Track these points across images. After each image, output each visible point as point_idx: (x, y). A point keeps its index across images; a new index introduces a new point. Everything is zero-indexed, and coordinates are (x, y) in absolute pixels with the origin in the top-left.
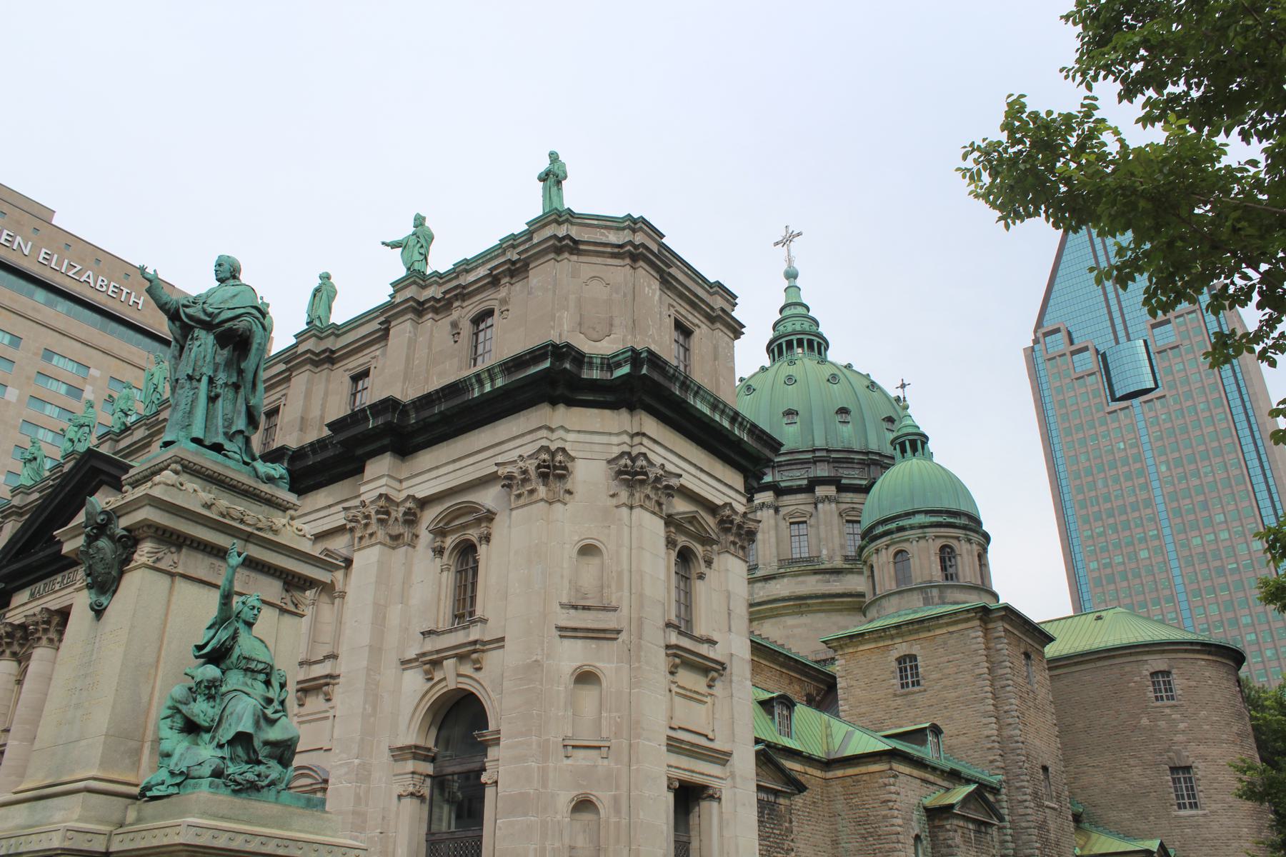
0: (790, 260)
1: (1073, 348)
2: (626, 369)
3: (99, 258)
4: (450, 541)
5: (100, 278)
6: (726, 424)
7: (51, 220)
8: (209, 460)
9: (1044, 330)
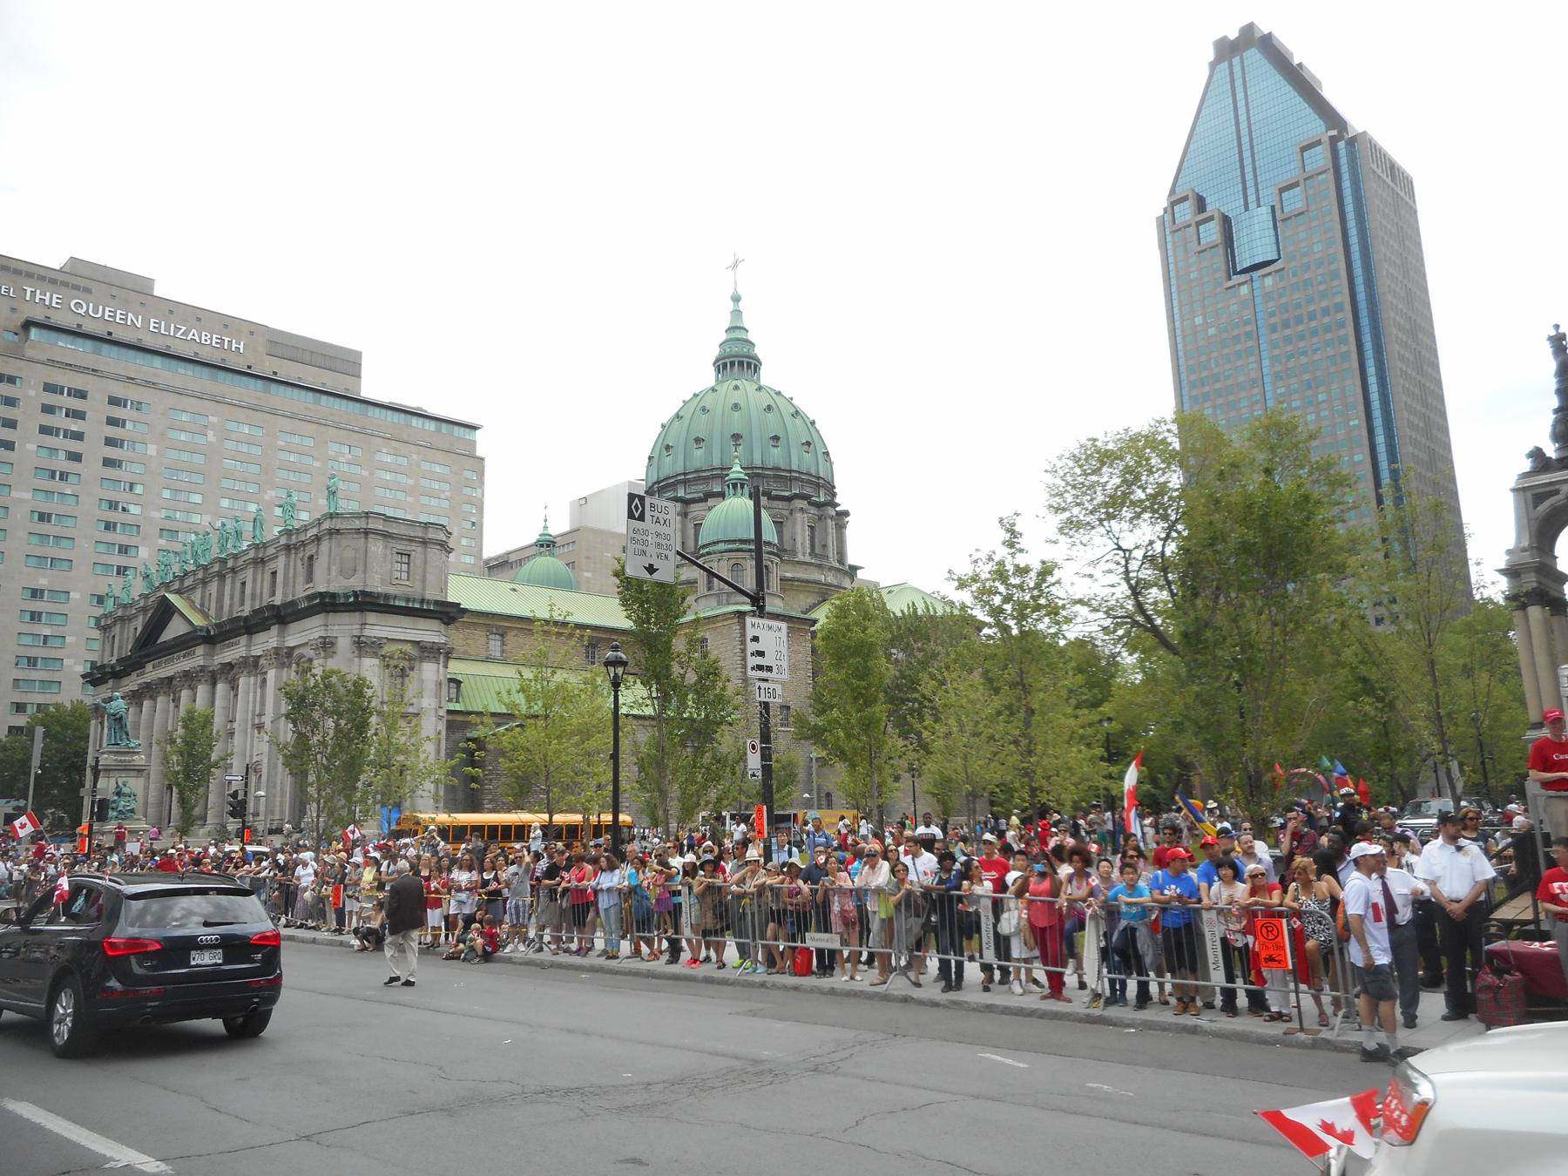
2: (352, 599)
3: (199, 317)
5: (204, 333)
6: (417, 606)
7: (153, 289)
8: (115, 749)
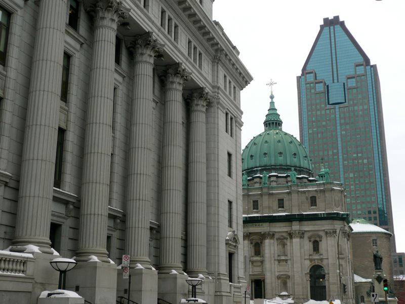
0: (272, 92)
1: (317, 81)
2: (346, 216)
4: (312, 240)
9: (307, 72)
